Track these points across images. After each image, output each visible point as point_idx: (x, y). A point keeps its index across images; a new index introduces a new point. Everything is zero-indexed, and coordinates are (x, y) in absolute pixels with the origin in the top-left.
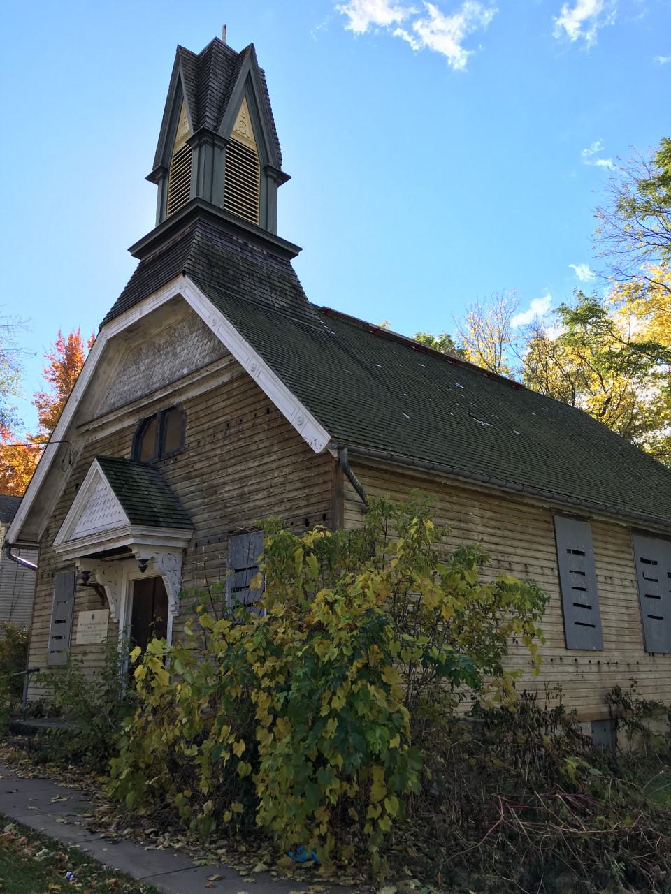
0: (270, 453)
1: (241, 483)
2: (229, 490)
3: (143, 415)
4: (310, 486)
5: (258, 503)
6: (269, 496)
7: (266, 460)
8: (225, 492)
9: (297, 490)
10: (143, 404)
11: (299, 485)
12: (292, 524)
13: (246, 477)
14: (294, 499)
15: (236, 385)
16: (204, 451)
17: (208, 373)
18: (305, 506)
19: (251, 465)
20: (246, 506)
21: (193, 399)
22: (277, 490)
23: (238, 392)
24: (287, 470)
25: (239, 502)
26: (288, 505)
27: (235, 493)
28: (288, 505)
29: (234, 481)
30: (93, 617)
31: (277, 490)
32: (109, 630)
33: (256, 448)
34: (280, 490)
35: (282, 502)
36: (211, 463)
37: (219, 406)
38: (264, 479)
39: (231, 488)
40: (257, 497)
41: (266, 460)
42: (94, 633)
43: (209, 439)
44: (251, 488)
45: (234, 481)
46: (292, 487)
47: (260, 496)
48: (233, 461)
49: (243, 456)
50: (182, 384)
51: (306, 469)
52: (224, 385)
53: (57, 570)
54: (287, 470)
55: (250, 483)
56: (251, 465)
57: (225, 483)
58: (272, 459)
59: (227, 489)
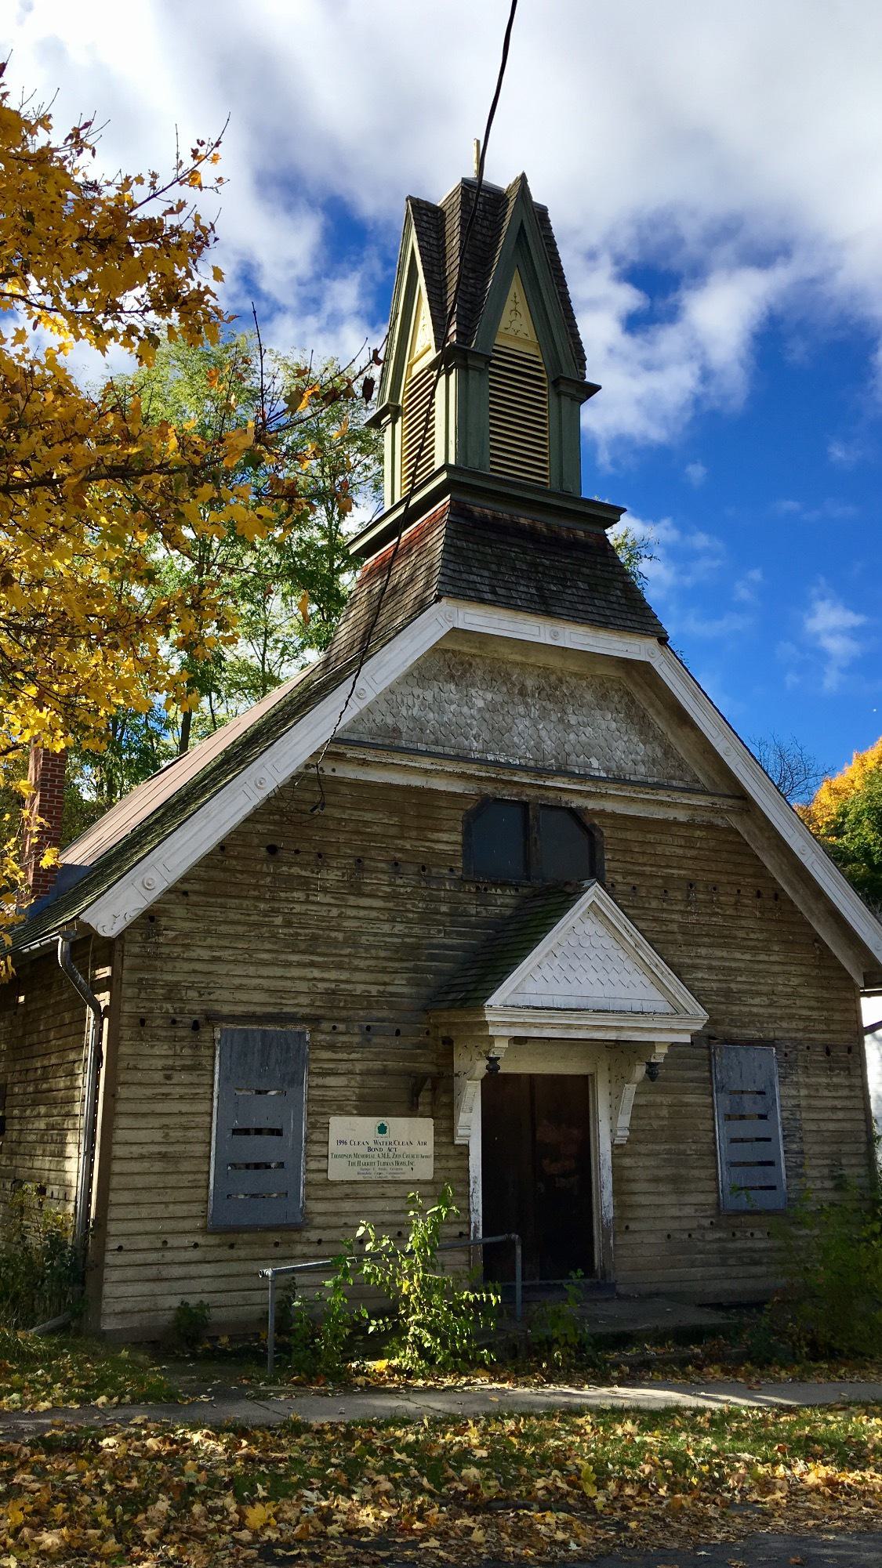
0: (768, 951)
1: (724, 975)
2: (703, 979)
3: (489, 789)
4: (827, 1010)
5: (755, 1010)
6: (769, 1006)
7: (762, 957)
8: (697, 979)
9: (811, 1008)
10: (516, 779)
11: (813, 1003)
12: (808, 1048)
13: (731, 969)
14: (808, 1018)
15: (698, 833)
16: (647, 905)
17: (668, 799)
18: (823, 1032)
19: (738, 956)
20: (735, 1008)
21: (613, 816)
22: (784, 1002)
23: (705, 846)
24: (795, 981)
25: (723, 1000)
26: (801, 1025)
27: (714, 985)
28: (801, 1025)
29: (710, 968)
30: (382, 1129)
31: (784, 1002)
32: (437, 1158)
33: (744, 936)
34: (788, 1002)
35: (791, 1017)
36: (664, 928)
37: (668, 851)
38: (762, 981)
39: (706, 977)
40: (751, 1001)
41: (762, 957)
42: (383, 1160)
43: (655, 892)
44: (740, 986)
45: (710, 968)
46: (804, 1003)
47: (757, 1001)
48: (706, 940)
49: (725, 940)
50: (616, 789)
51: (822, 987)
52: (676, 823)
53: (212, 1018)
54: (795, 981)
55: (739, 979)
56: (738, 956)
57: (695, 967)
58: (772, 958)
59: (700, 975)
